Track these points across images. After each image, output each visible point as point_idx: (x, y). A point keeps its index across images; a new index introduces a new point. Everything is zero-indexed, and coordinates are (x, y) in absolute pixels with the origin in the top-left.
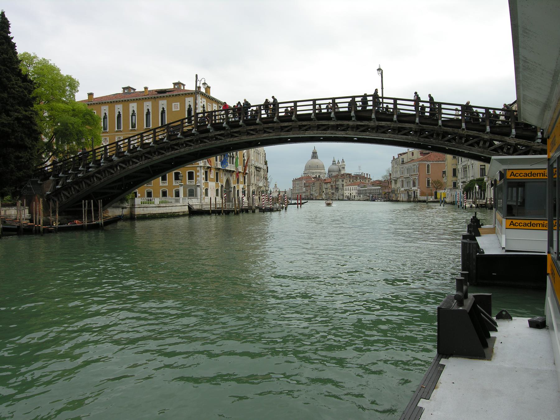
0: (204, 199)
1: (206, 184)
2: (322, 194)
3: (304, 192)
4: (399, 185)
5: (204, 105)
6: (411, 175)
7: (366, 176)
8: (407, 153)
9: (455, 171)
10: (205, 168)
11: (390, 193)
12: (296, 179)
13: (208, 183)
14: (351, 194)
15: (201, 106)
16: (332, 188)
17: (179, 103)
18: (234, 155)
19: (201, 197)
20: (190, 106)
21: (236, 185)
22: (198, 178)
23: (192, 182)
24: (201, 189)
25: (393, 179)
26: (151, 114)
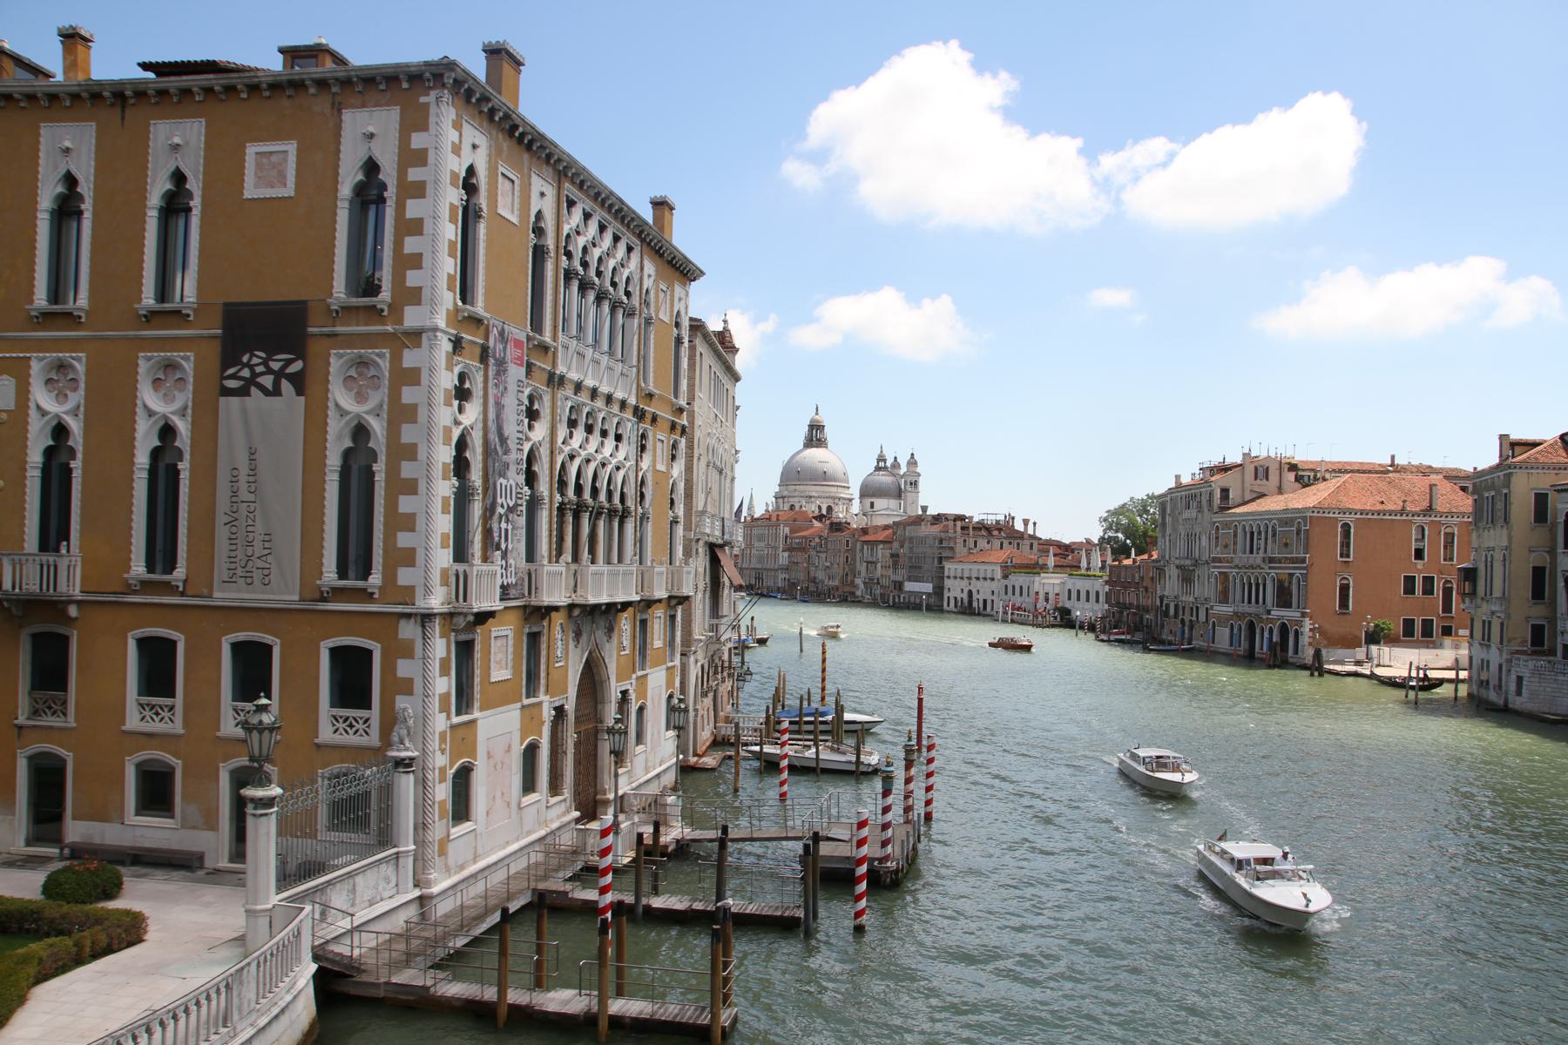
0: (443, 852)
1: (463, 737)
2: (853, 582)
3: (787, 569)
4: (1205, 588)
5: (471, 171)
6: (1272, 560)
7: (1019, 526)
8: (1241, 465)
9: (1538, 573)
10: (461, 622)
11: (1147, 610)
13: (473, 722)
14: (970, 593)
15: (454, 175)
16: (895, 564)
17: (291, 148)
18: (630, 503)
19: (420, 842)
20: (371, 167)
21: (630, 685)
22: (401, 702)
23: (361, 726)
24: (423, 783)
25: (1177, 562)
26: (87, 217)
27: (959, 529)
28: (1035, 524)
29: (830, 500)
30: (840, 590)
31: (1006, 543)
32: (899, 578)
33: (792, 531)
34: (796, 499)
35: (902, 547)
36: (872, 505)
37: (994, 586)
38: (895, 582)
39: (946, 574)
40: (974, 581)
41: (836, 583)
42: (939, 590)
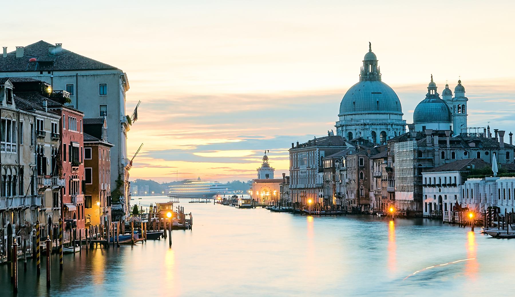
2: (367, 196)
12: (299, 146)
14: (440, 197)
27: (436, 142)
28: (511, 134)
29: (383, 127)
30: (356, 203)
31: (482, 153)
32: (391, 189)
33: (326, 154)
34: (353, 127)
35: (394, 161)
36: (424, 128)
37: (456, 190)
38: (390, 193)
39: (424, 183)
40: (442, 188)
41: (353, 197)
42: (419, 197)
